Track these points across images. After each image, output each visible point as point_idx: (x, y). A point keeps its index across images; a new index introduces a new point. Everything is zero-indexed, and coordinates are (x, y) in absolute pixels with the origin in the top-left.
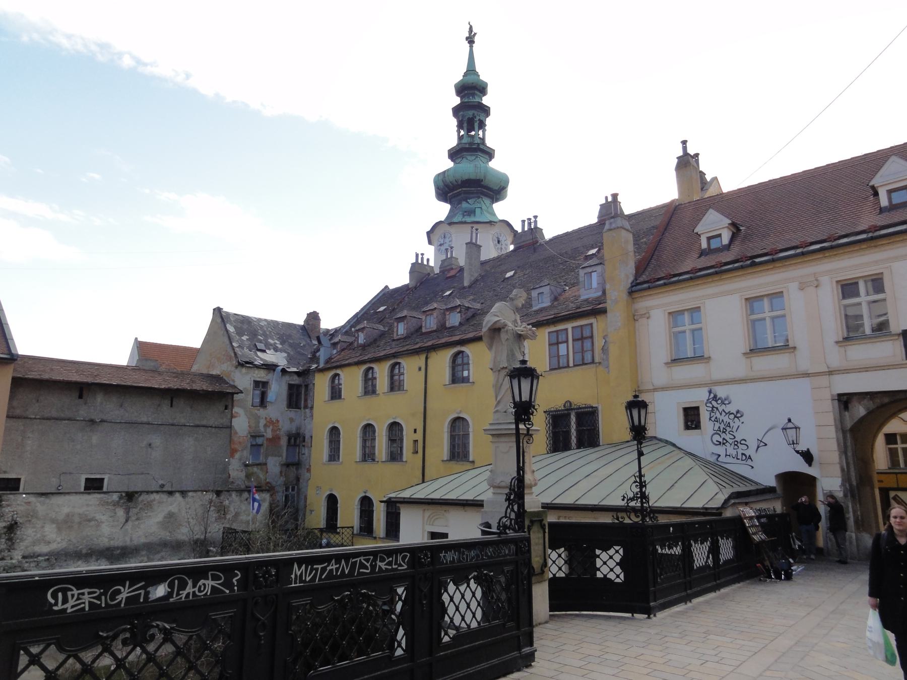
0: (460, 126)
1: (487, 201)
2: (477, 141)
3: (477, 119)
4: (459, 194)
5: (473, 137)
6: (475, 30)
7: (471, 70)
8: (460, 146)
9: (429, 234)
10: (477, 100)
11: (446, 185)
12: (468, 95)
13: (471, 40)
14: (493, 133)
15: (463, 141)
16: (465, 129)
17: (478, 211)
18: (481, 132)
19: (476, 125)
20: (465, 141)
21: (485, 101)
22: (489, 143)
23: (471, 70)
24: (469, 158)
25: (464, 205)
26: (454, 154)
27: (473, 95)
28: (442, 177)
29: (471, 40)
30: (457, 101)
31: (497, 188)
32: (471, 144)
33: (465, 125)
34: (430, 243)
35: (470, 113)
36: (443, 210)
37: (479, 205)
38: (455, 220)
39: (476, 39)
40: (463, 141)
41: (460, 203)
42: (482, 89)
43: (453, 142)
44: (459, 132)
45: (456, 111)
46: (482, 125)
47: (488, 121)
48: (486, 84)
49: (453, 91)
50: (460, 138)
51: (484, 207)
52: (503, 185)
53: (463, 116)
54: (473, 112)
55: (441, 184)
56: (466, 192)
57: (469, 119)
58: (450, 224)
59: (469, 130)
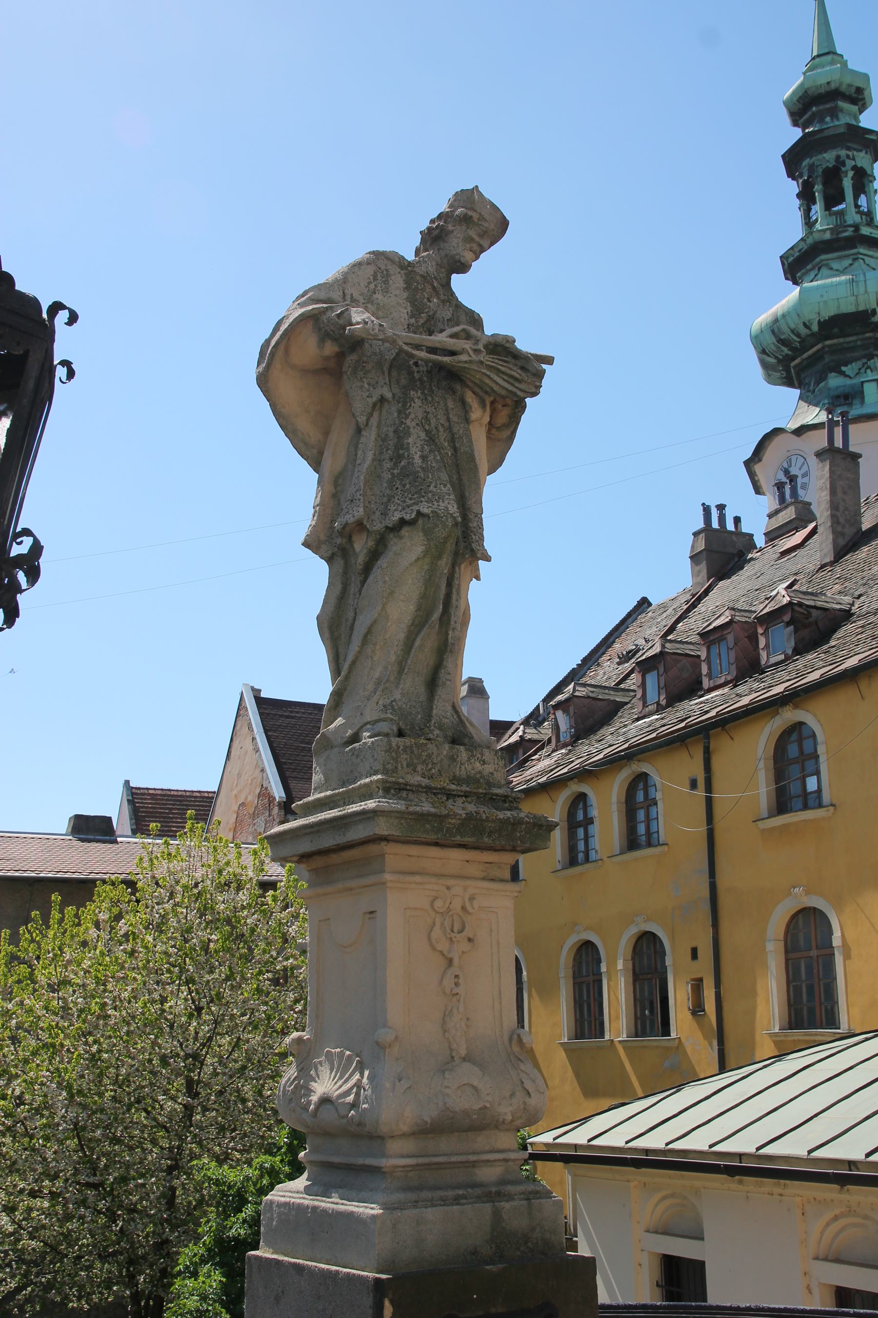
0: (806, 196)
2: (852, 217)
3: (850, 164)
4: (817, 357)
5: (842, 213)
8: (810, 241)
9: (748, 464)
10: (844, 119)
11: (783, 342)
12: (819, 117)
18: (863, 200)
19: (847, 184)
24: (835, 265)
25: (834, 381)
26: (797, 265)
30: (798, 133)
33: (818, 188)
34: (758, 490)
35: (829, 157)
36: (788, 408)
40: (818, 226)
41: (822, 378)
42: (858, 97)
45: (793, 160)
49: (786, 120)
50: (809, 223)
53: (812, 168)
55: (770, 341)
56: (834, 350)
59: (833, 198)
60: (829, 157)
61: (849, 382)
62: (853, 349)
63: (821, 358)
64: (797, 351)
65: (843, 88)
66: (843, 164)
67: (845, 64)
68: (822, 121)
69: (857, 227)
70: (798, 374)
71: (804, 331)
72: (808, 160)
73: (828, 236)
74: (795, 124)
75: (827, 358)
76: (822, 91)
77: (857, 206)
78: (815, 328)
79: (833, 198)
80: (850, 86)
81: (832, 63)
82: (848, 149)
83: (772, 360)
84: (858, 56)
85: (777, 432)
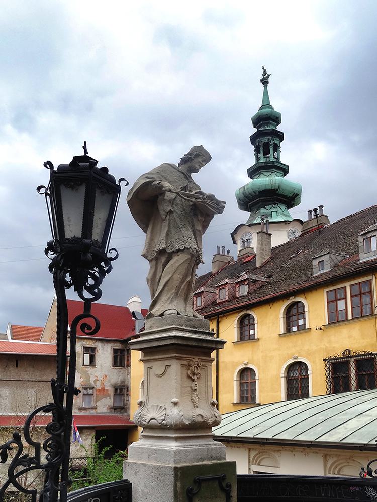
0: (257, 151)
1: (283, 207)
2: (272, 159)
5: (269, 157)
6: (268, 73)
7: (266, 104)
8: (258, 166)
9: (233, 235)
10: (271, 127)
13: (265, 82)
14: (286, 156)
15: (260, 161)
16: (262, 151)
17: (274, 214)
20: (262, 160)
21: (279, 128)
22: (284, 159)
23: (266, 104)
24: (265, 174)
25: (262, 211)
27: (268, 124)
28: (242, 190)
29: (265, 82)
30: (256, 130)
31: (291, 196)
32: (265, 163)
33: (262, 148)
35: (265, 139)
37: (275, 210)
38: (255, 222)
39: (270, 80)
42: (276, 119)
43: (251, 162)
44: (257, 156)
45: (253, 139)
46: (277, 148)
47: (282, 144)
48: (280, 114)
50: (258, 159)
51: (279, 211)
52: (295, 192)
54: (268, 137)
57: (265, 143)
58: (250, 226)
59: (266, 152)
60: (265, 139)
61: (267, 211)
62: (270, 201)
63: (259, 203)
64: (250, 200)
65: (272, 117)
66: (270, 141)
67: (273, 109)
68: (264, 127)
69: (273, 162)
70: (250, 208)
71: (254, 194)
72: (258, 139)
73: (264, 165)
74: (255, 127)
75: (260, 204)
76: (265, 117)
77: (274, 156)
78: (257, 193)
79: (266, 152)
80: (274, 116)
81: (269, 108)
82: (272, 137)
83: (242, 202)
84: (277, 106)
85: (242, 225)
